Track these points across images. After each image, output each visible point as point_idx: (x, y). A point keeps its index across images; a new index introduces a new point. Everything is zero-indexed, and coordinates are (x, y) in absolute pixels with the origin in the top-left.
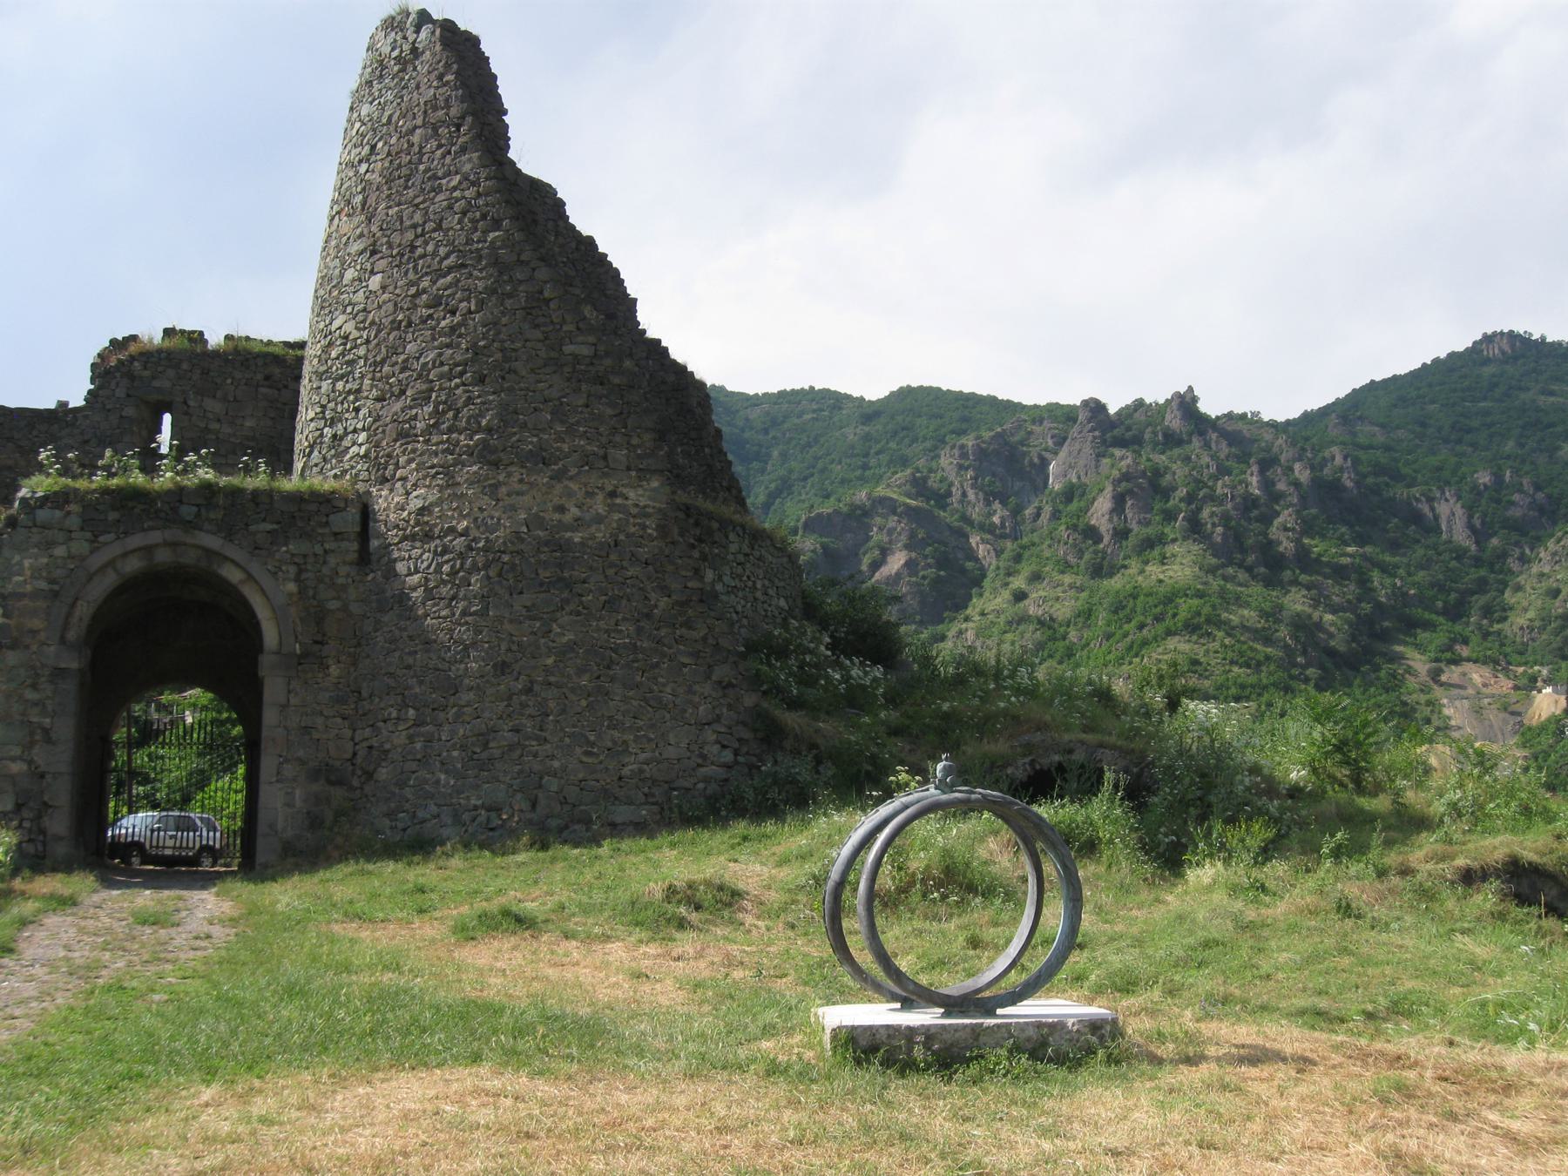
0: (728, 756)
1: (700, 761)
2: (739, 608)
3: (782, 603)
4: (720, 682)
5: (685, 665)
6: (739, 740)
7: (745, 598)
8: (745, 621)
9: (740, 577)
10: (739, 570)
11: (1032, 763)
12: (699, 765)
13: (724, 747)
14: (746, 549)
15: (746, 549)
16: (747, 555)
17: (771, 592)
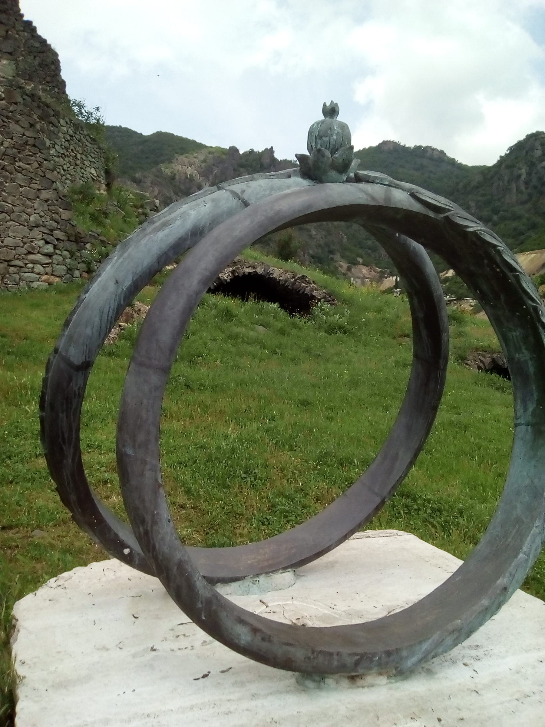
0: (49, 249)
1: (31, 250)
2: (65, 167)
3: (93, 171)
4: (46, 201)
5: (21, 186)
6: (58, 239)
7: (70, 162)
8: (69, 176)
9: (67, 149)
10: (67, 144)
11: (233, 272)
12: (30, 253)
13: (47, 243)
14: (71, 132)
15: (71, 132)
16: (71, 136)
17: (85, 162)
